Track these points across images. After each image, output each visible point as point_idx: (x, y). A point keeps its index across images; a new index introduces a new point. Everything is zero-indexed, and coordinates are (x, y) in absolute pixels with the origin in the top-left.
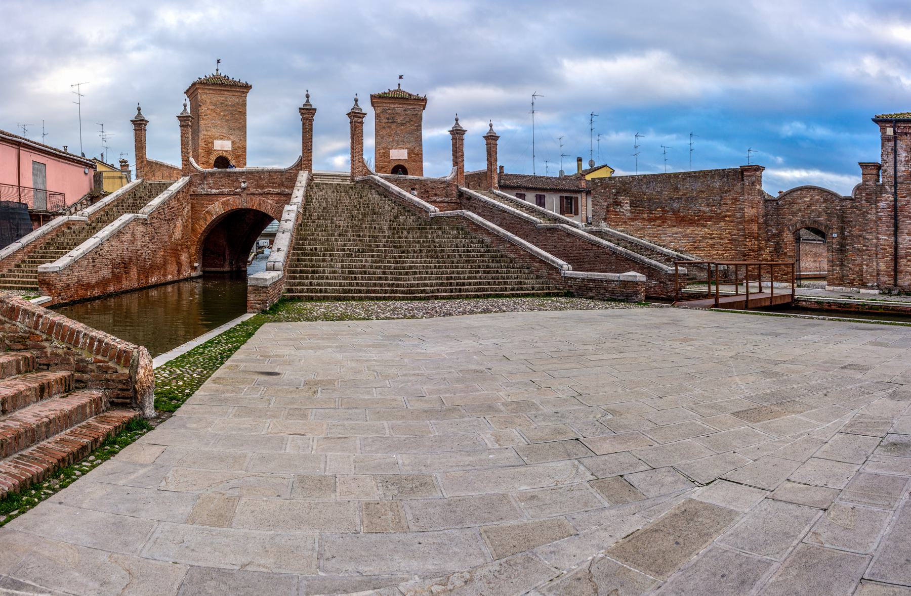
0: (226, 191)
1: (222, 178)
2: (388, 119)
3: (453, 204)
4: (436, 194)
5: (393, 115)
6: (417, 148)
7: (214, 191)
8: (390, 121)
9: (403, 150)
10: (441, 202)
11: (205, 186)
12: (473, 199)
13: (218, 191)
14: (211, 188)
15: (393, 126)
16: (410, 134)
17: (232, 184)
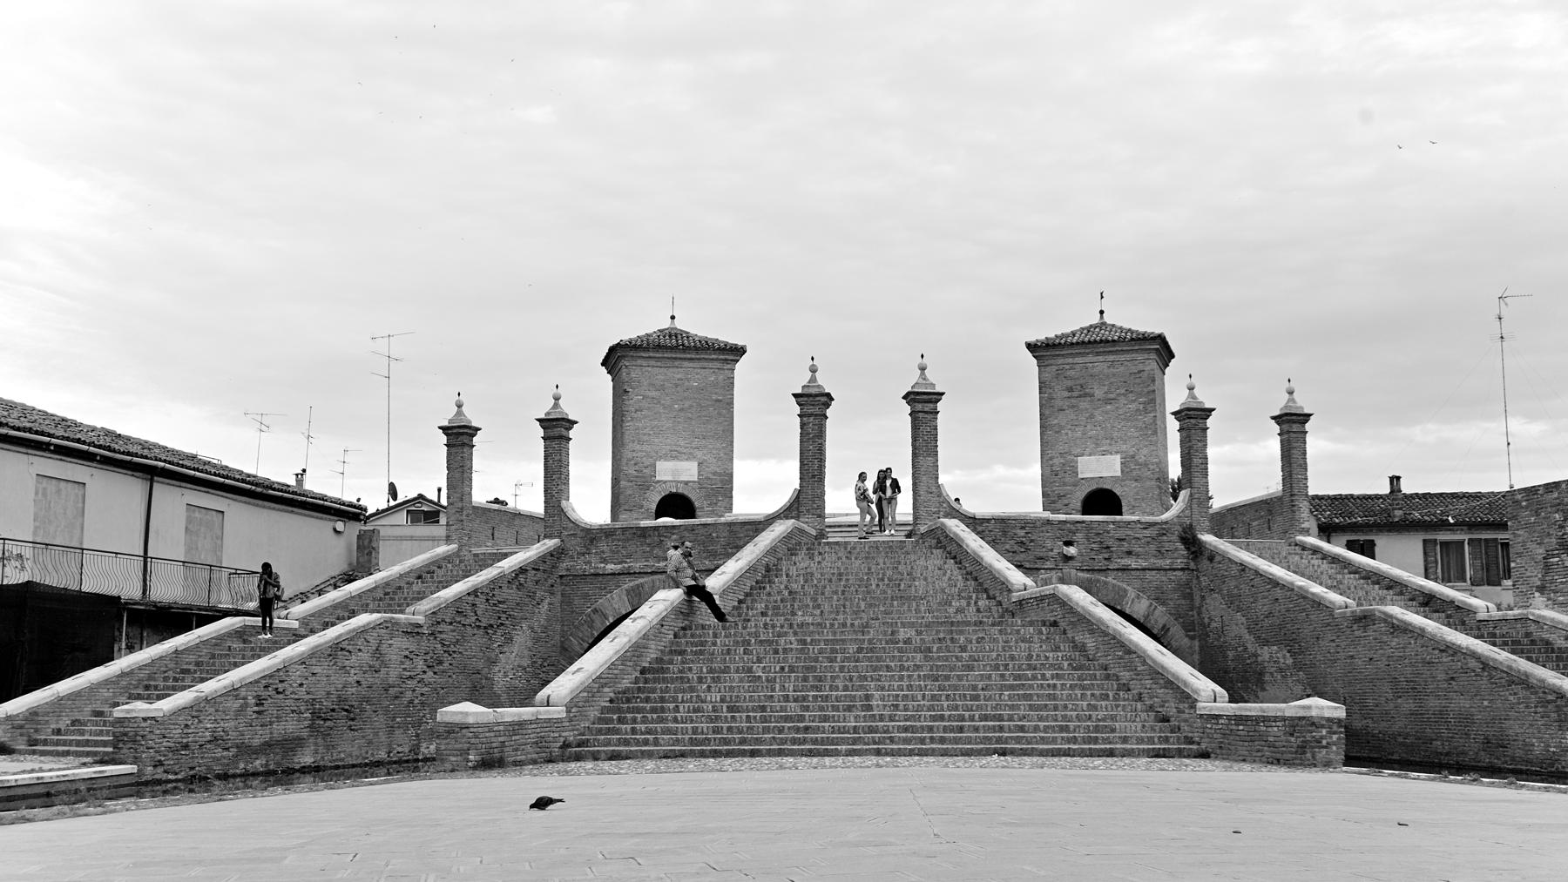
0: (637, 566)
1: (628, 540)
2: (1070, 389)
3: (1179, 573)
4: (1129, 553)
5: (1082, 381)
6: (1145, 451)
7: (610, 567)
8: (1075, 394)
10: (1144, 569)
11: (594, 560)
12: (1218, 558)
13: (619, 567)
14: (604, 561)
15: (1084, 404)
16: (1128, 420)
17: (652, 550)
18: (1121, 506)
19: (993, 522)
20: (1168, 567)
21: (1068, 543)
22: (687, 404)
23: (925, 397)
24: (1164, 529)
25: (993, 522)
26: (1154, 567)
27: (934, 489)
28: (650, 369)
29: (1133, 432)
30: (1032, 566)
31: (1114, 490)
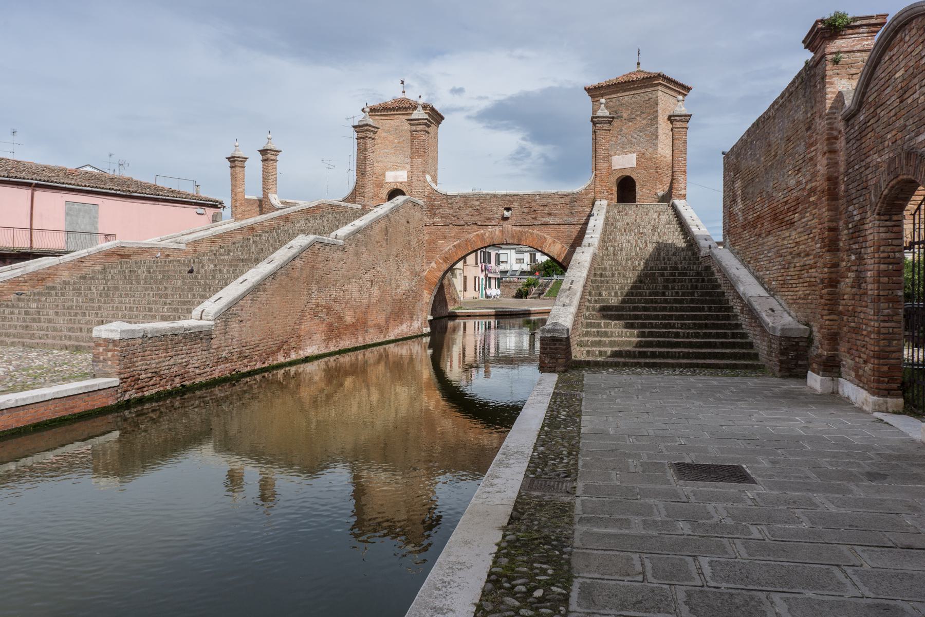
6: (650, 150)
9: (630, 155)
16: (640, 131)
18: (635, 186)
19: (459, 197)
20: (576, 223)
21: (508, 209)
22: (402, 139)
23: (416, 122)
24: (575, 198)
25: (459, 197)
26: (566, 223)
27: (421, 178)
28: (382, 121)
29: (644, 139)
30: (482, 224)
31: (632, 176)
